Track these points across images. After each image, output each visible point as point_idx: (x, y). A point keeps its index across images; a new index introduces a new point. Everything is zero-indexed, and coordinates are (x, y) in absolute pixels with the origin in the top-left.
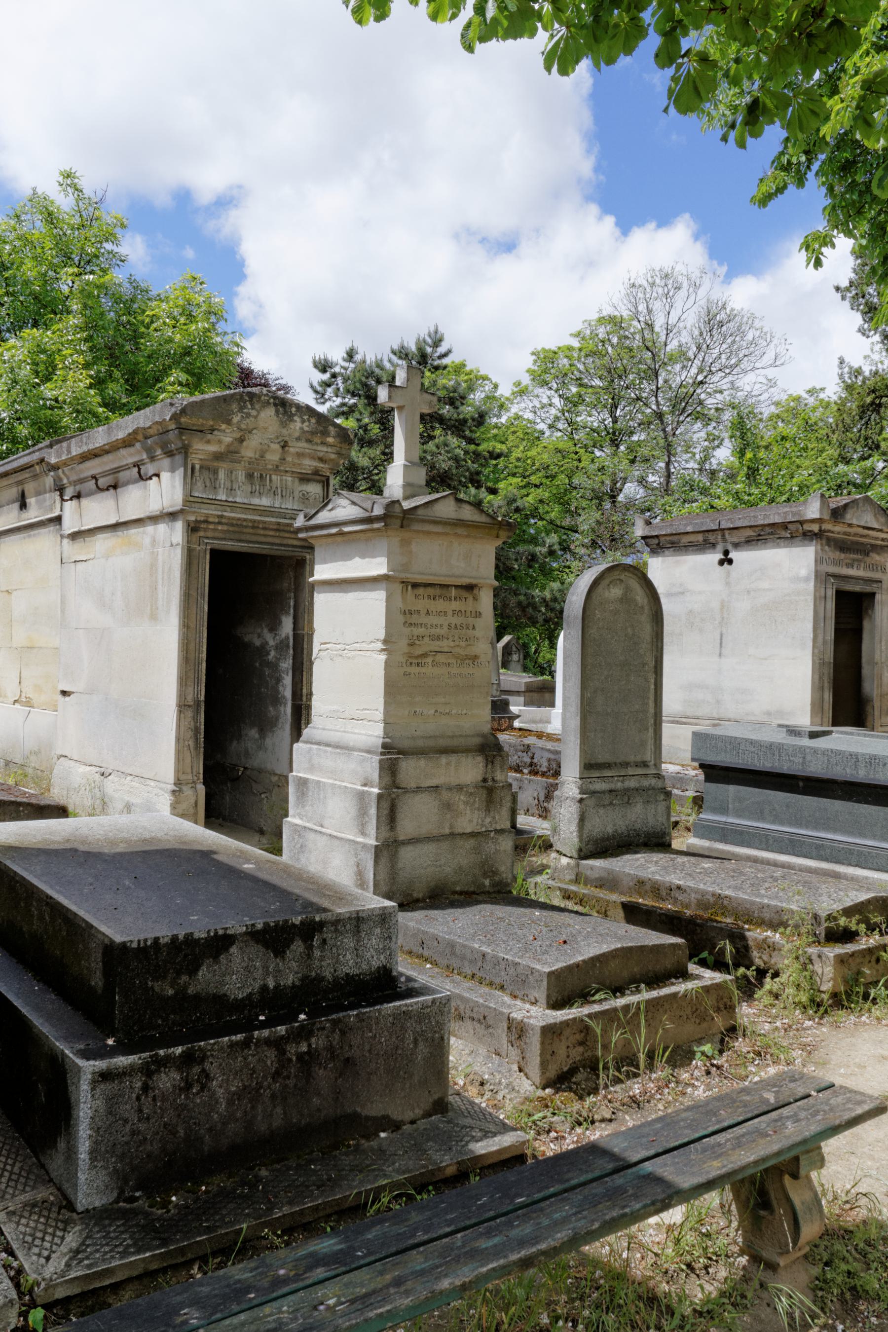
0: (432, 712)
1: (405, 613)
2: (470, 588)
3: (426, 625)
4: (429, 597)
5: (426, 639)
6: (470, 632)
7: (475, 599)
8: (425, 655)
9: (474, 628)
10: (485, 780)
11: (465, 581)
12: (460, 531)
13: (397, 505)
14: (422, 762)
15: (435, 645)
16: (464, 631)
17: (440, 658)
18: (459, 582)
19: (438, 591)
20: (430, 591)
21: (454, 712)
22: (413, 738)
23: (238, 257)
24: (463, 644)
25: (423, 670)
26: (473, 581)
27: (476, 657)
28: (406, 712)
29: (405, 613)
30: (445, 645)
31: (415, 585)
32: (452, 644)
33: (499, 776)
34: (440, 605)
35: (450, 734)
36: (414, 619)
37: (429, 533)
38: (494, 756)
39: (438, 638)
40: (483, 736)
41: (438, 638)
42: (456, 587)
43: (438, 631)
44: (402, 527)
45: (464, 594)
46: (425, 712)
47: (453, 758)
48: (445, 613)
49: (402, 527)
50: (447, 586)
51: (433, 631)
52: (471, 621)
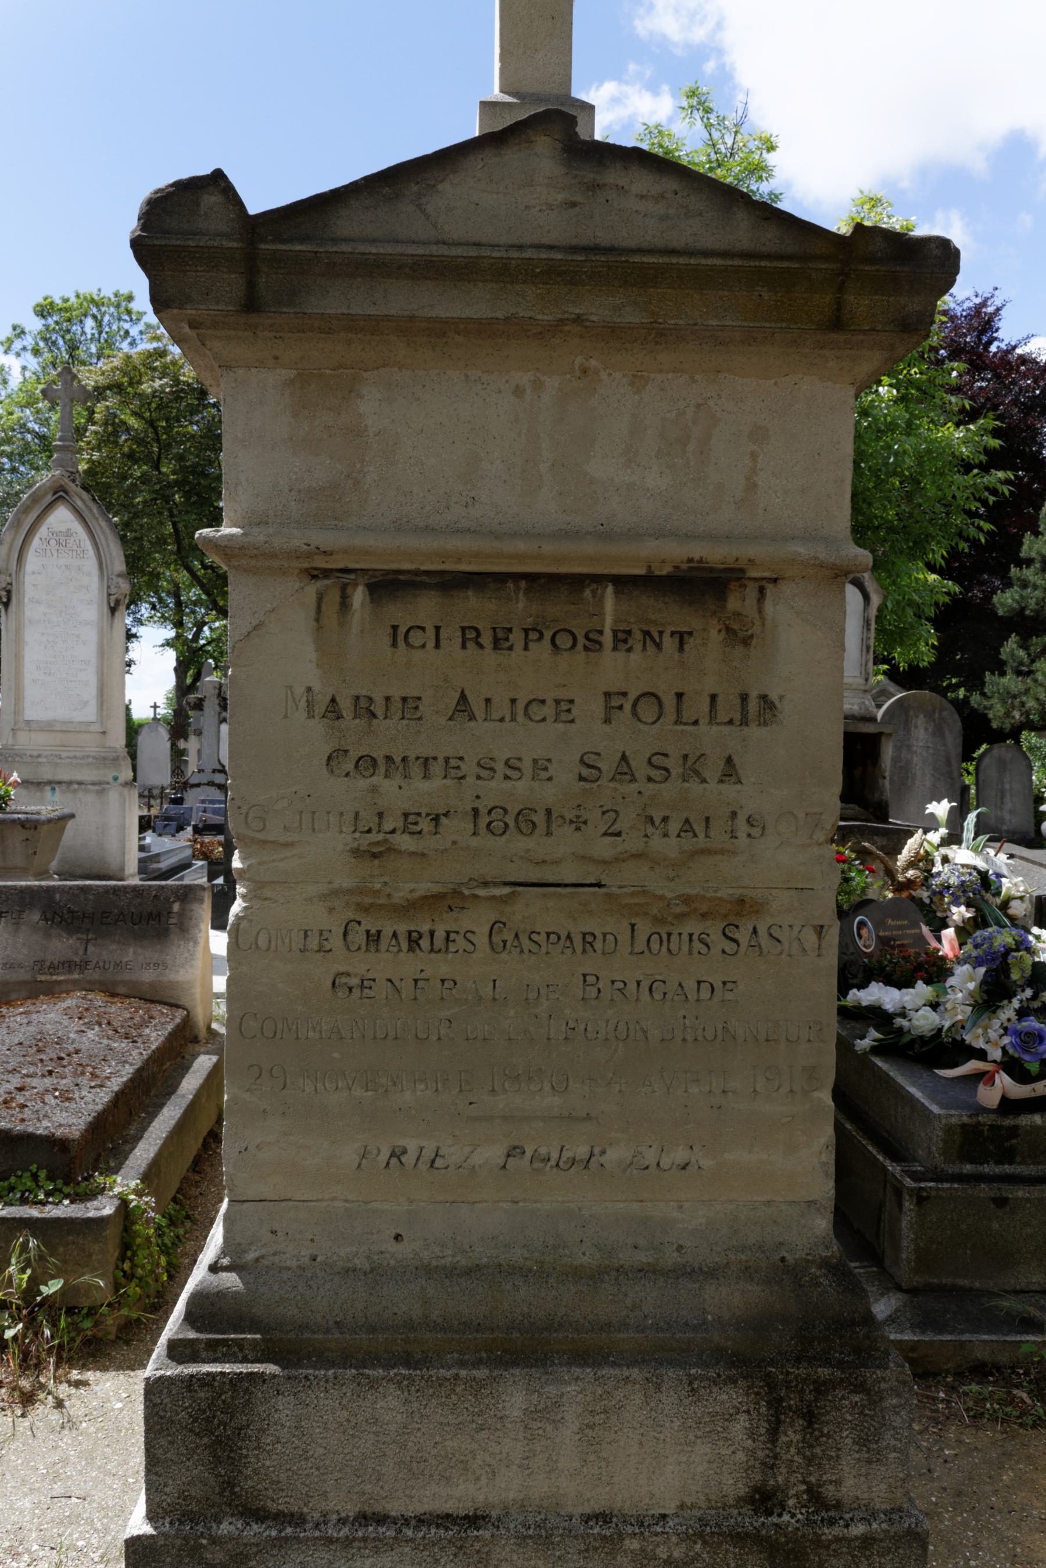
0: (494, 1153)
1: (333, 710)
2: (703, 586)
3: (451, 766)
4: (470, 636)
5: (457, 828)
6: (712, 792)
7: (738, 636)
8: (450, 899)
9: (730, 771)
10: (764, 1499)
11: (670, 554)
12: (597, 307)
13: (211, 199)
14: (389, 1405)
15: (509, 854)
16: (669, 790)
17: (534, 911)
18: (635, 558)
19: (521, 608)
20: (477, 608)
21: (613, 1155)
22: (376, 1273)
23: (678, 52)
24: (670, 847)
25: (442, 966)
26: (716, 555)
27: (743, 906)
28: (349, 1154)
29: (333, 710)
30: (561, 851)
31: (388, 585)
32: (605, 848)
33: (853, 1481)
34: (533, 669)
35: (587, 1258)
36: (389, 736)
37: (439, 331)
38: (821, 1388)
39: (524, 820)
40: (788, 1273)
41: (524, 820)
42: (623, 583)
43: (523, 789)
44: (251, 304)
45: (672, 615)
46: (453, 1153)
47: (574, 1390)
48: (564, 708)
49: (251, 304)
50: (576, 582)
51: (494, 790)
52: (712, 739)
